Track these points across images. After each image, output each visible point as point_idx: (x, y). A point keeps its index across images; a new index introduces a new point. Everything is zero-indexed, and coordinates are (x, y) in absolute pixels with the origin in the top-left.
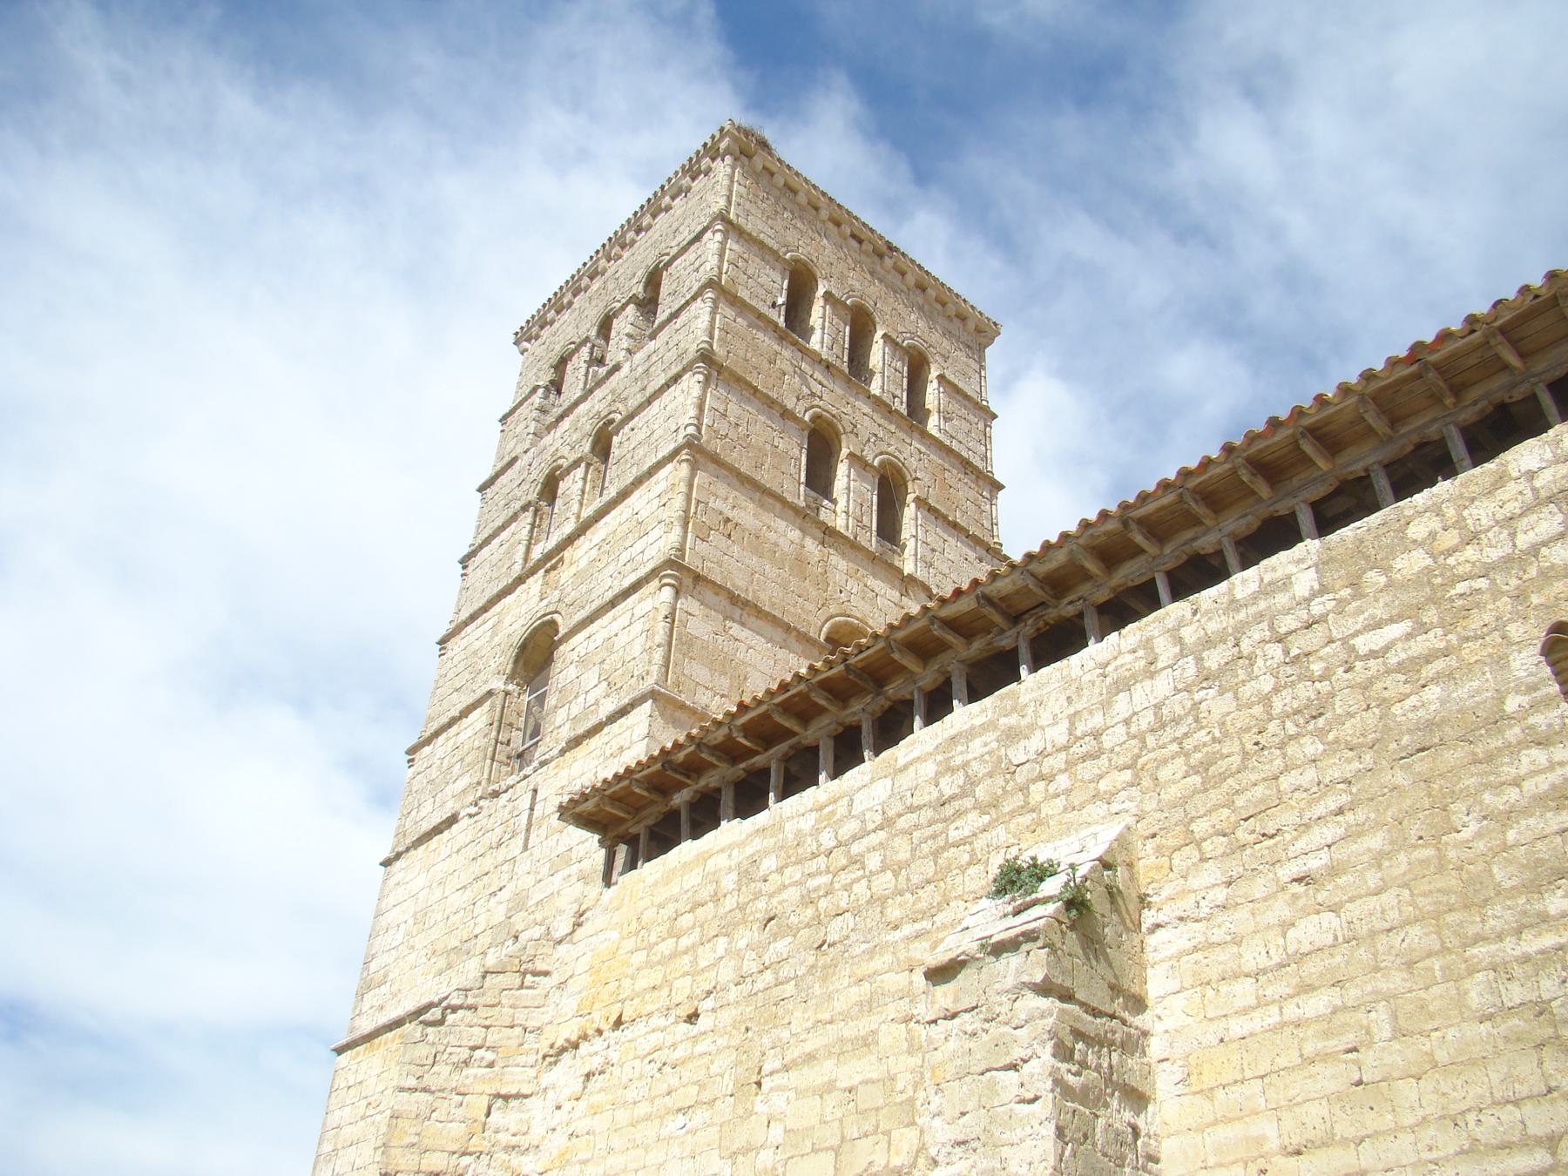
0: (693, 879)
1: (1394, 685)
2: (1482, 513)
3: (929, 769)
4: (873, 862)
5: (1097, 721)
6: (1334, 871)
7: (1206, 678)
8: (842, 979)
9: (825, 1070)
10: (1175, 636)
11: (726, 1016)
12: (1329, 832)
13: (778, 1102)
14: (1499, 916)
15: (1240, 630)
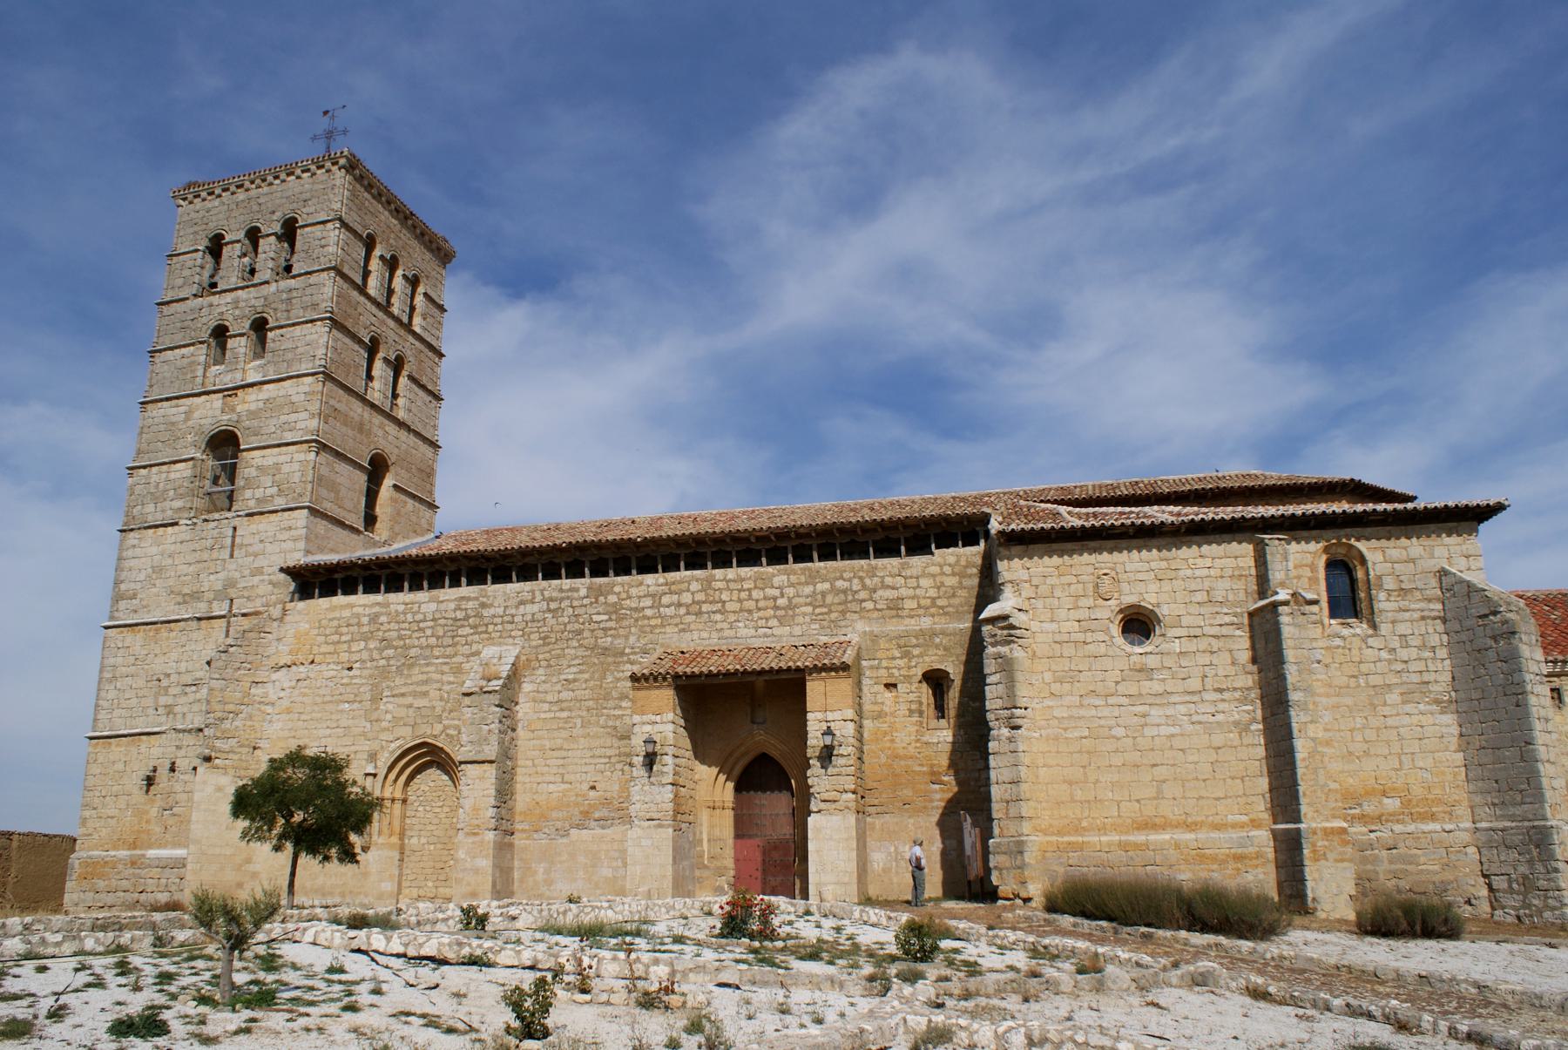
0: (346, 613)
1: (600, 634)
2: (634, 591)
3: (452, 606)
4: (429, 632)
5: (513, 611)
6: (575, 680)
7: (549, 610)
8: (416, 670)
9: (409, 700)
10: (542, 591)
11: (366, 672)
12: (574, 669)
13: (390, 707)
14: (611, 704)
15: (562, 599)
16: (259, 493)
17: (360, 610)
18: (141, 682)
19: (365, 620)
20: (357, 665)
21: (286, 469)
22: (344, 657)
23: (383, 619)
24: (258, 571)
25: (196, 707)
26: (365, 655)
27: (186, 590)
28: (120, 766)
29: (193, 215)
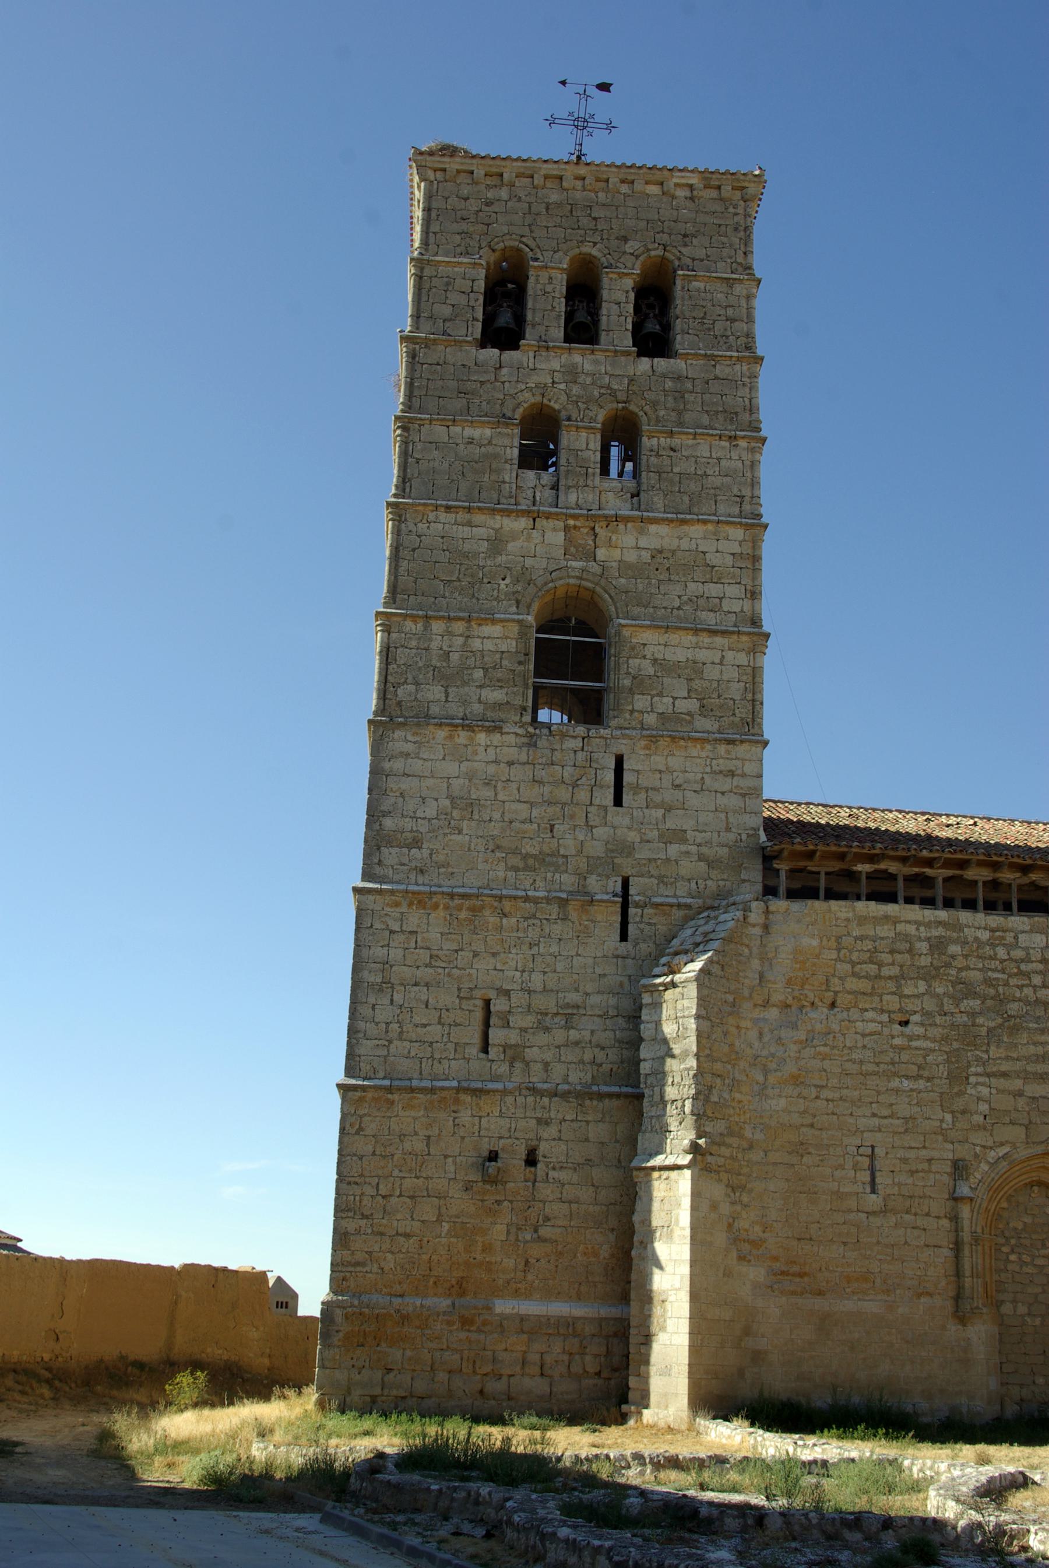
0: (885, 931)
4: (1037, 980)
8: (1024, 1037)
9: (1017, 1084)
11: (933, 1032)
16: (664, 704)
17: (911, 929)
18: (446, 998)
19: (923, 947)
20: (915, 1018)
21: (712, 673)
22: (892, 1002)
23: (954, 949)
24: (679, 836)
25: (568, 1055)
26: (930, 1005)
27: (528, 848)
28: (420, 1146)
29: (453, 201)
